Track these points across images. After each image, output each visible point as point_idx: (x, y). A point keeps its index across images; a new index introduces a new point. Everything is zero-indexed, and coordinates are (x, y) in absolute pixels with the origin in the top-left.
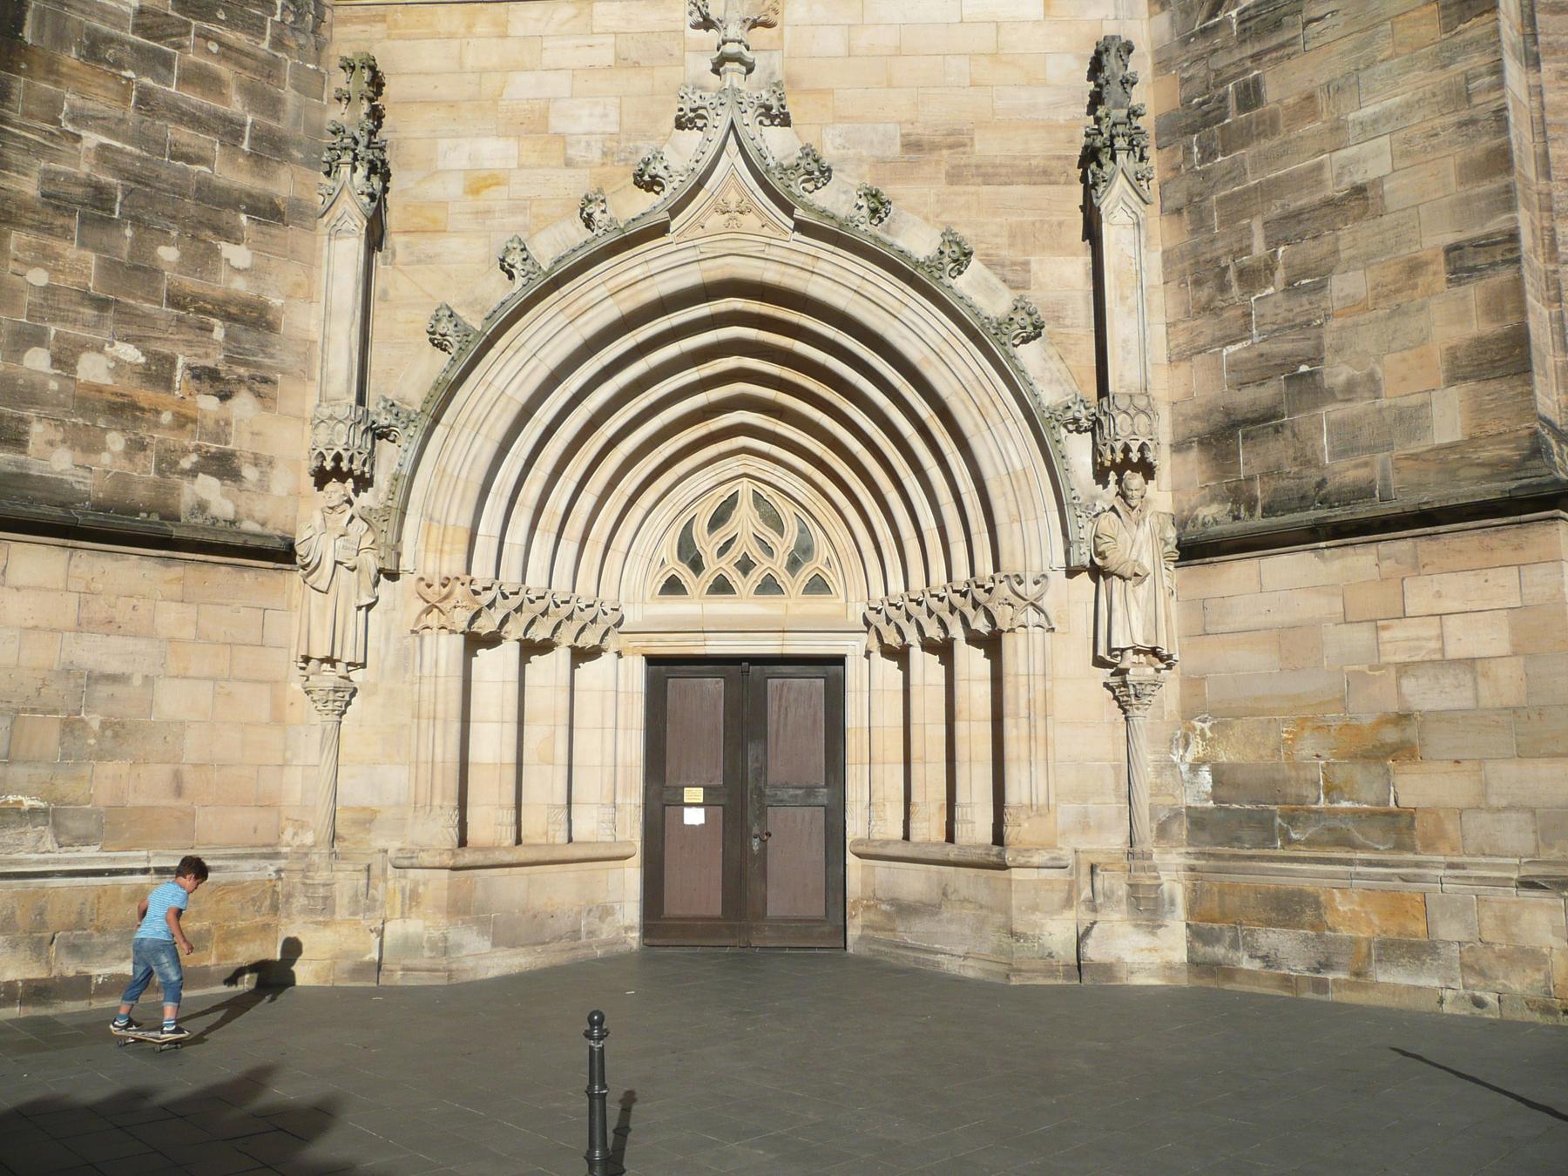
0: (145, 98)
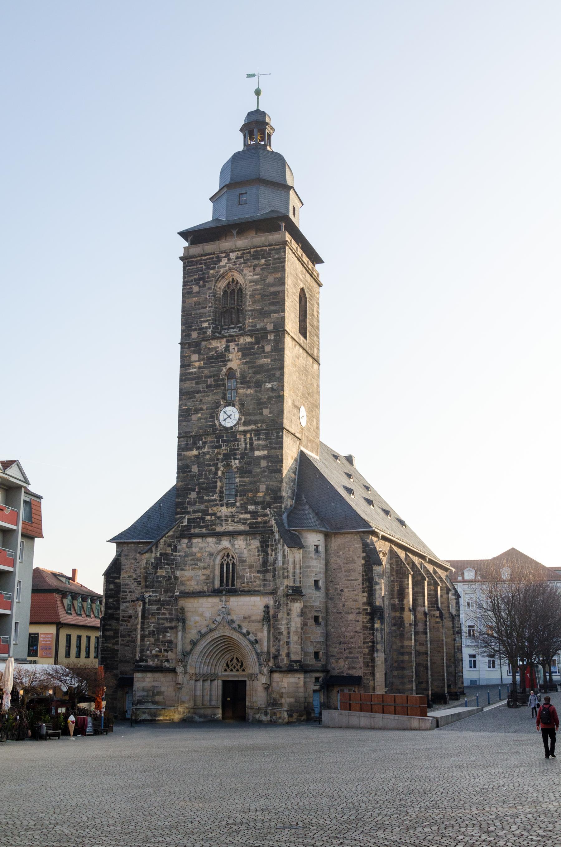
0: (158, 618)
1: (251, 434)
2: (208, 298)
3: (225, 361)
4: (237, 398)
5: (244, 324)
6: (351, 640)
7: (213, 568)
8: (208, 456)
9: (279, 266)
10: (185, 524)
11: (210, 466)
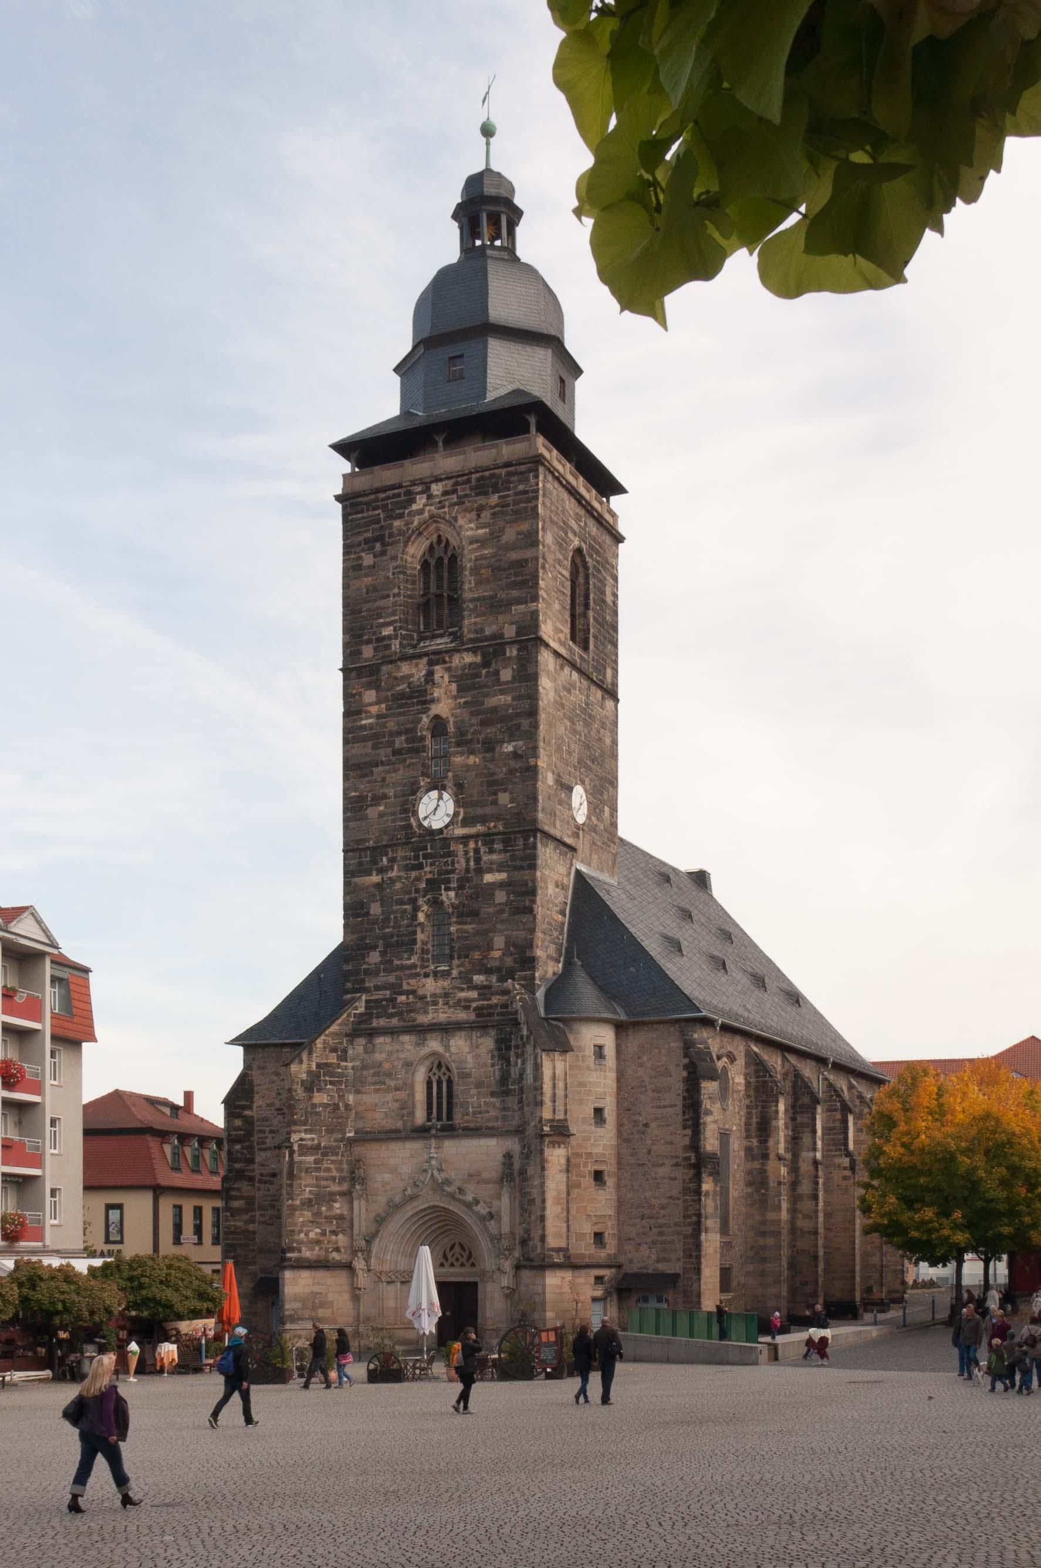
0: (317, 1178)
1: (476, 842)
3: (425, 702)
5: (461, 628)
6: (662, 1212)
8: (398, 886)
9: (527, 507)
10: (362, 1010)
11: (402, 903)
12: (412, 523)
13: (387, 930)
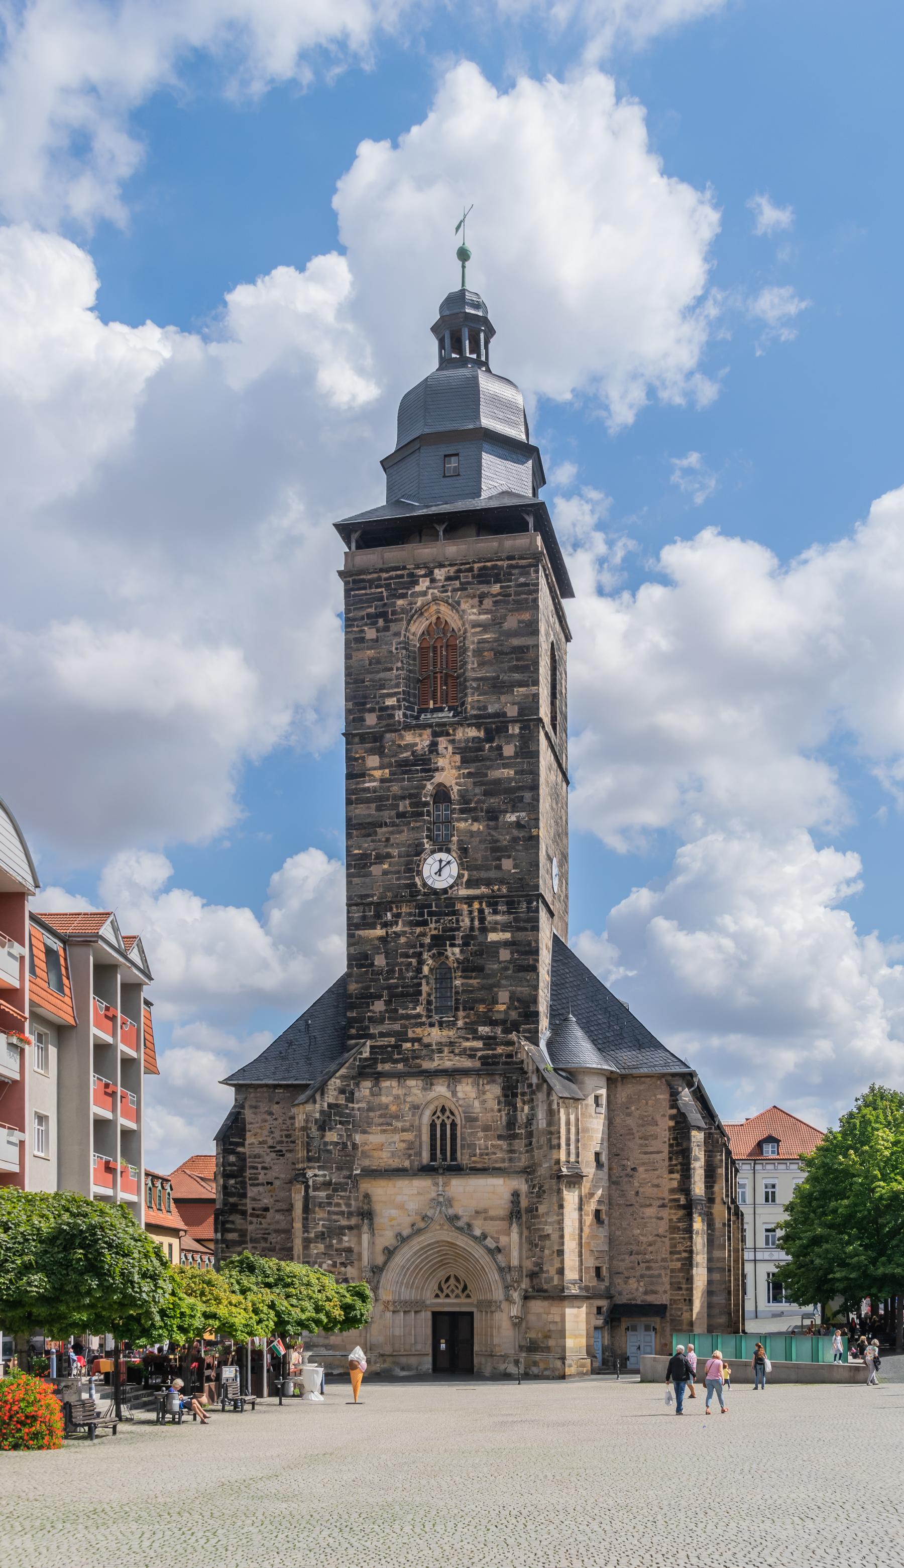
1: (481, 903)
2: (394, 651)
3: (429, 770)
4: (455, 839)
7: (419, 1129)
8: (403, 940)
9: (526, 599)
10: (366, 1054)
12: (416, 603)
13: (392, 981)
